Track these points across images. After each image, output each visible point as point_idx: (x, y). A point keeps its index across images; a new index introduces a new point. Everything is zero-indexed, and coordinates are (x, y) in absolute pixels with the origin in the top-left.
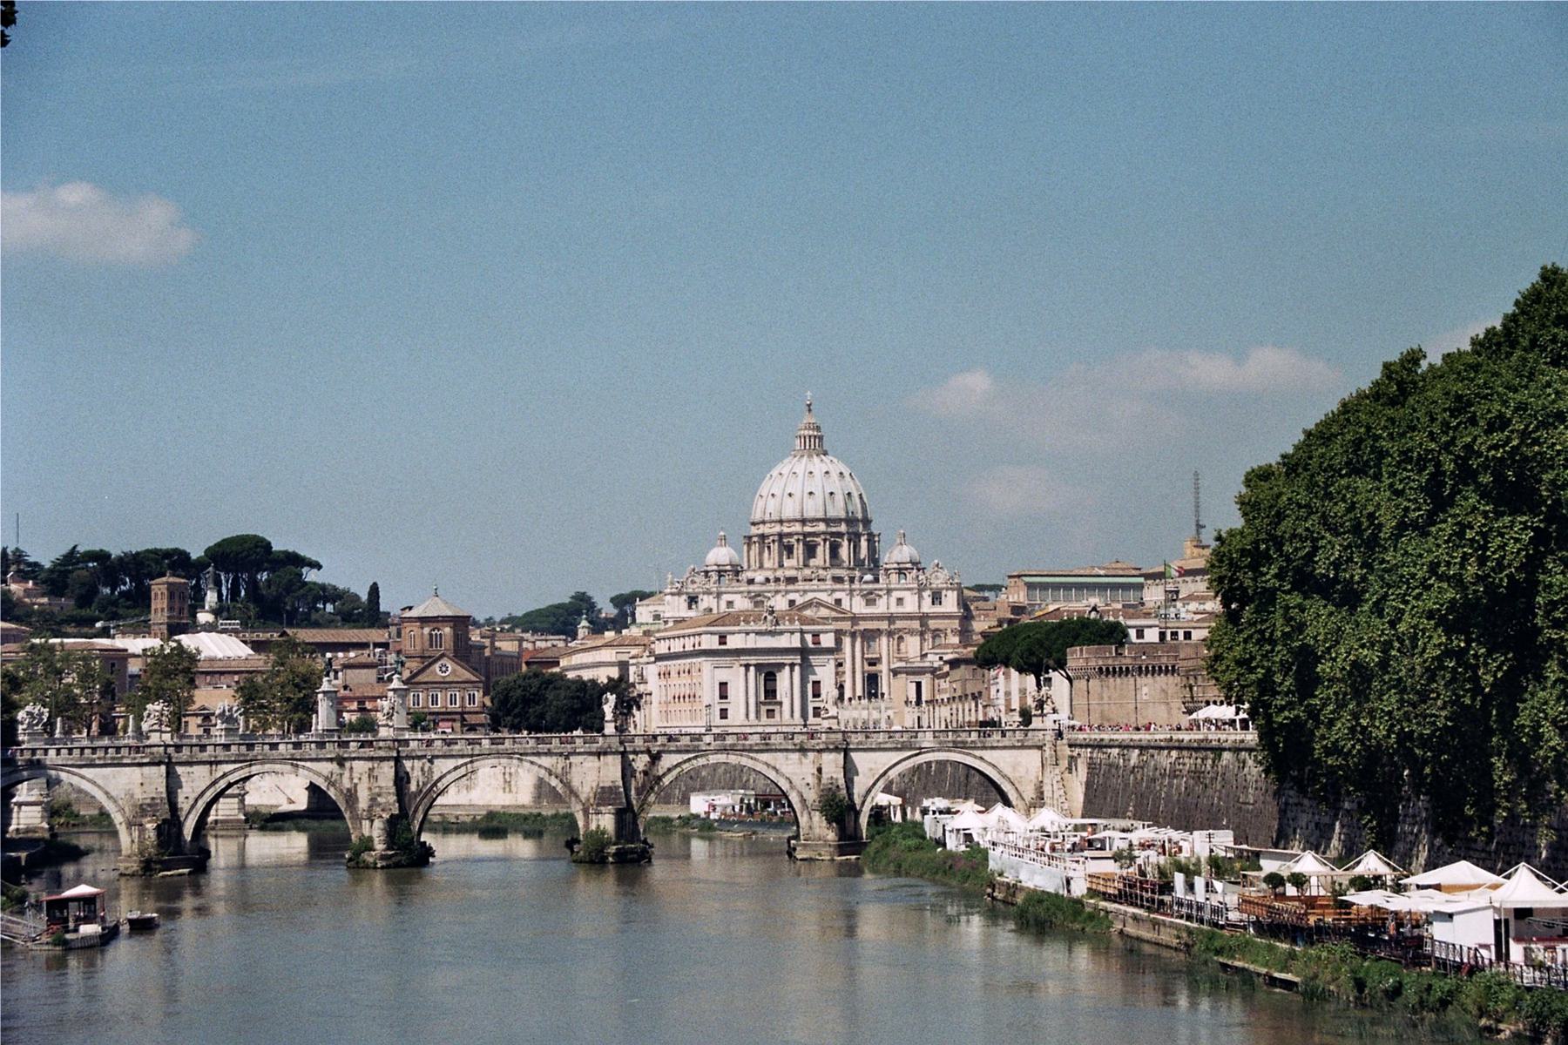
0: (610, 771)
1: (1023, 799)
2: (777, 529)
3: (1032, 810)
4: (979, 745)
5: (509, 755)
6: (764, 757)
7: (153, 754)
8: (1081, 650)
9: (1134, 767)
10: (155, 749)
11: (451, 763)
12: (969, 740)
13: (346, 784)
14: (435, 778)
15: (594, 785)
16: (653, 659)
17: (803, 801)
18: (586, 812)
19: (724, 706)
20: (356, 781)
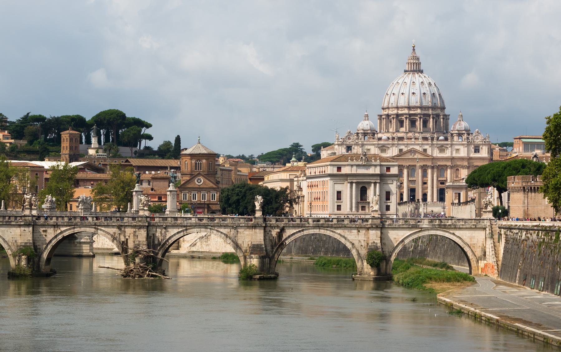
0: (258, 237)
1: (475, 256)
2: (395, 112)
3: (480, 261)
4: (452, 227)
5: (206, 226)
6: (339, 231)
7: (26, 220)
8: (514, 178)
9: (523, 240)
10: (27, 218)
11: (175, 231)
12: (448, 224)
13: (122, 239)
14: (168, 237)
15: (250, 243)
16: (305, 178)
17: (359, 254)
18: (245, 258)
19: (339, 204)
20: (127, 237)
